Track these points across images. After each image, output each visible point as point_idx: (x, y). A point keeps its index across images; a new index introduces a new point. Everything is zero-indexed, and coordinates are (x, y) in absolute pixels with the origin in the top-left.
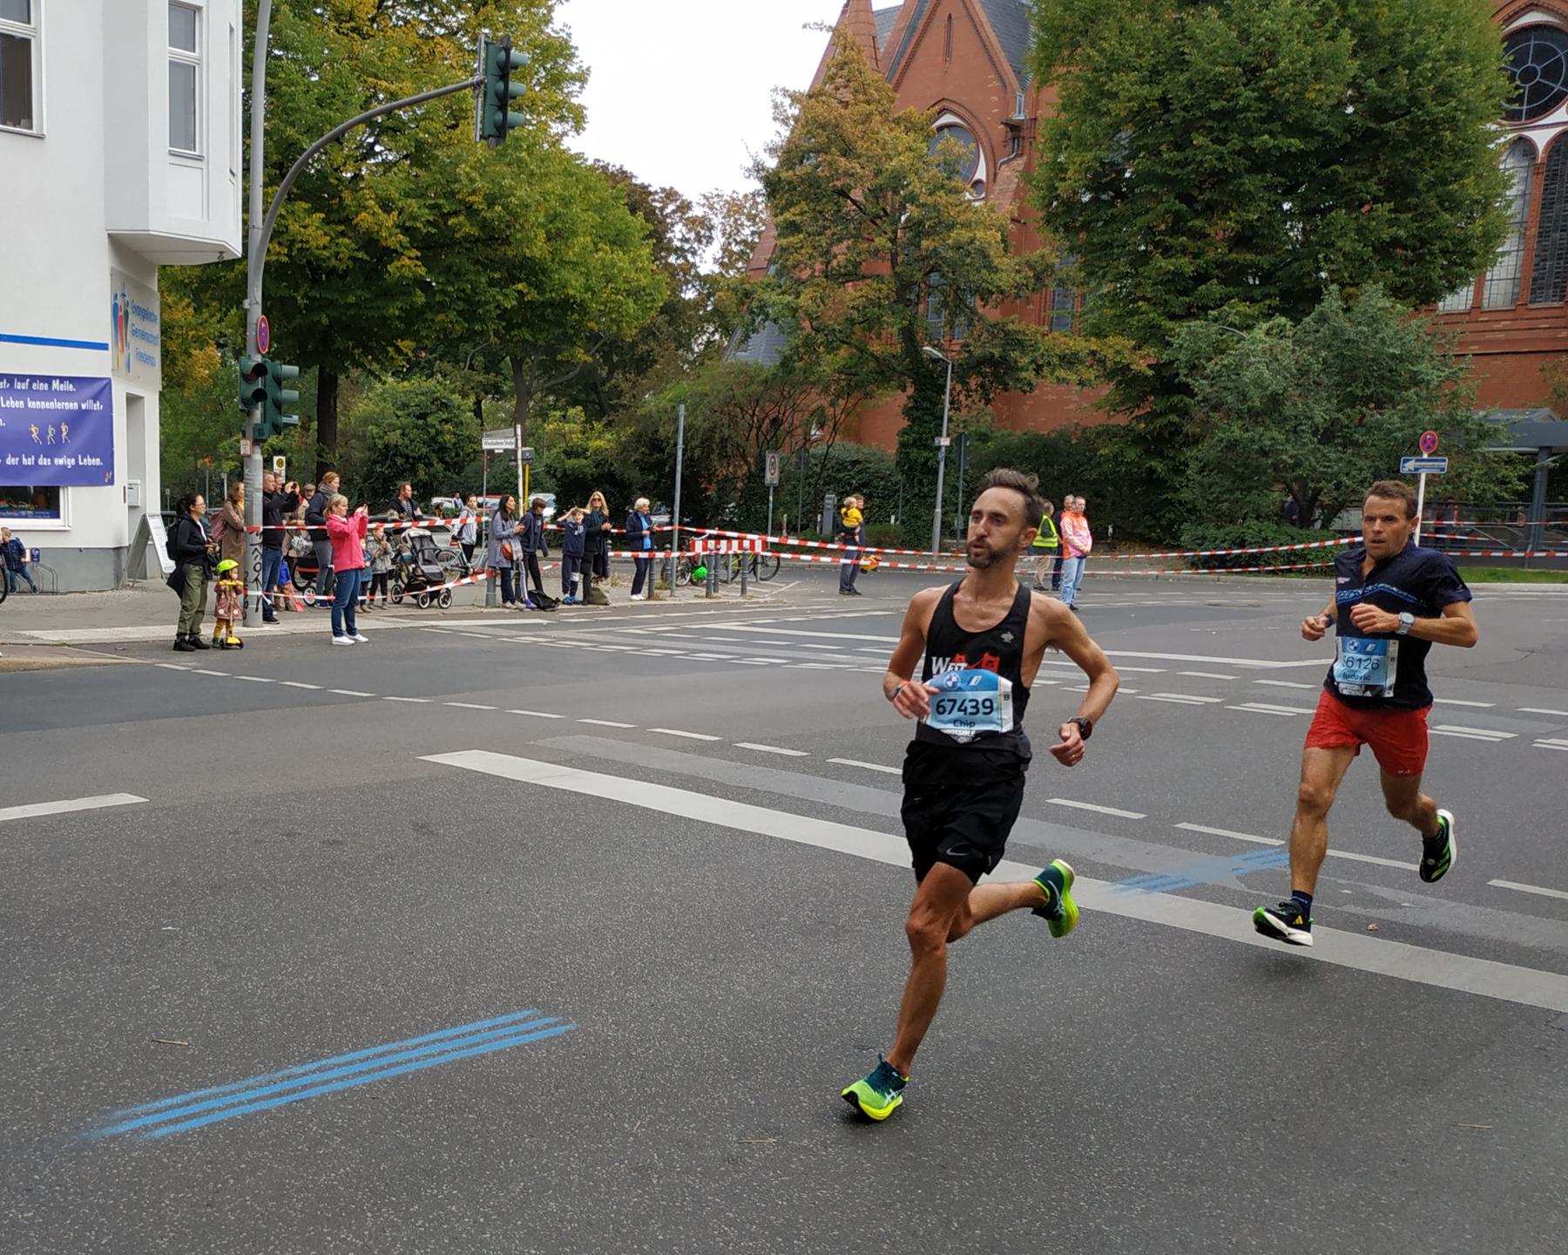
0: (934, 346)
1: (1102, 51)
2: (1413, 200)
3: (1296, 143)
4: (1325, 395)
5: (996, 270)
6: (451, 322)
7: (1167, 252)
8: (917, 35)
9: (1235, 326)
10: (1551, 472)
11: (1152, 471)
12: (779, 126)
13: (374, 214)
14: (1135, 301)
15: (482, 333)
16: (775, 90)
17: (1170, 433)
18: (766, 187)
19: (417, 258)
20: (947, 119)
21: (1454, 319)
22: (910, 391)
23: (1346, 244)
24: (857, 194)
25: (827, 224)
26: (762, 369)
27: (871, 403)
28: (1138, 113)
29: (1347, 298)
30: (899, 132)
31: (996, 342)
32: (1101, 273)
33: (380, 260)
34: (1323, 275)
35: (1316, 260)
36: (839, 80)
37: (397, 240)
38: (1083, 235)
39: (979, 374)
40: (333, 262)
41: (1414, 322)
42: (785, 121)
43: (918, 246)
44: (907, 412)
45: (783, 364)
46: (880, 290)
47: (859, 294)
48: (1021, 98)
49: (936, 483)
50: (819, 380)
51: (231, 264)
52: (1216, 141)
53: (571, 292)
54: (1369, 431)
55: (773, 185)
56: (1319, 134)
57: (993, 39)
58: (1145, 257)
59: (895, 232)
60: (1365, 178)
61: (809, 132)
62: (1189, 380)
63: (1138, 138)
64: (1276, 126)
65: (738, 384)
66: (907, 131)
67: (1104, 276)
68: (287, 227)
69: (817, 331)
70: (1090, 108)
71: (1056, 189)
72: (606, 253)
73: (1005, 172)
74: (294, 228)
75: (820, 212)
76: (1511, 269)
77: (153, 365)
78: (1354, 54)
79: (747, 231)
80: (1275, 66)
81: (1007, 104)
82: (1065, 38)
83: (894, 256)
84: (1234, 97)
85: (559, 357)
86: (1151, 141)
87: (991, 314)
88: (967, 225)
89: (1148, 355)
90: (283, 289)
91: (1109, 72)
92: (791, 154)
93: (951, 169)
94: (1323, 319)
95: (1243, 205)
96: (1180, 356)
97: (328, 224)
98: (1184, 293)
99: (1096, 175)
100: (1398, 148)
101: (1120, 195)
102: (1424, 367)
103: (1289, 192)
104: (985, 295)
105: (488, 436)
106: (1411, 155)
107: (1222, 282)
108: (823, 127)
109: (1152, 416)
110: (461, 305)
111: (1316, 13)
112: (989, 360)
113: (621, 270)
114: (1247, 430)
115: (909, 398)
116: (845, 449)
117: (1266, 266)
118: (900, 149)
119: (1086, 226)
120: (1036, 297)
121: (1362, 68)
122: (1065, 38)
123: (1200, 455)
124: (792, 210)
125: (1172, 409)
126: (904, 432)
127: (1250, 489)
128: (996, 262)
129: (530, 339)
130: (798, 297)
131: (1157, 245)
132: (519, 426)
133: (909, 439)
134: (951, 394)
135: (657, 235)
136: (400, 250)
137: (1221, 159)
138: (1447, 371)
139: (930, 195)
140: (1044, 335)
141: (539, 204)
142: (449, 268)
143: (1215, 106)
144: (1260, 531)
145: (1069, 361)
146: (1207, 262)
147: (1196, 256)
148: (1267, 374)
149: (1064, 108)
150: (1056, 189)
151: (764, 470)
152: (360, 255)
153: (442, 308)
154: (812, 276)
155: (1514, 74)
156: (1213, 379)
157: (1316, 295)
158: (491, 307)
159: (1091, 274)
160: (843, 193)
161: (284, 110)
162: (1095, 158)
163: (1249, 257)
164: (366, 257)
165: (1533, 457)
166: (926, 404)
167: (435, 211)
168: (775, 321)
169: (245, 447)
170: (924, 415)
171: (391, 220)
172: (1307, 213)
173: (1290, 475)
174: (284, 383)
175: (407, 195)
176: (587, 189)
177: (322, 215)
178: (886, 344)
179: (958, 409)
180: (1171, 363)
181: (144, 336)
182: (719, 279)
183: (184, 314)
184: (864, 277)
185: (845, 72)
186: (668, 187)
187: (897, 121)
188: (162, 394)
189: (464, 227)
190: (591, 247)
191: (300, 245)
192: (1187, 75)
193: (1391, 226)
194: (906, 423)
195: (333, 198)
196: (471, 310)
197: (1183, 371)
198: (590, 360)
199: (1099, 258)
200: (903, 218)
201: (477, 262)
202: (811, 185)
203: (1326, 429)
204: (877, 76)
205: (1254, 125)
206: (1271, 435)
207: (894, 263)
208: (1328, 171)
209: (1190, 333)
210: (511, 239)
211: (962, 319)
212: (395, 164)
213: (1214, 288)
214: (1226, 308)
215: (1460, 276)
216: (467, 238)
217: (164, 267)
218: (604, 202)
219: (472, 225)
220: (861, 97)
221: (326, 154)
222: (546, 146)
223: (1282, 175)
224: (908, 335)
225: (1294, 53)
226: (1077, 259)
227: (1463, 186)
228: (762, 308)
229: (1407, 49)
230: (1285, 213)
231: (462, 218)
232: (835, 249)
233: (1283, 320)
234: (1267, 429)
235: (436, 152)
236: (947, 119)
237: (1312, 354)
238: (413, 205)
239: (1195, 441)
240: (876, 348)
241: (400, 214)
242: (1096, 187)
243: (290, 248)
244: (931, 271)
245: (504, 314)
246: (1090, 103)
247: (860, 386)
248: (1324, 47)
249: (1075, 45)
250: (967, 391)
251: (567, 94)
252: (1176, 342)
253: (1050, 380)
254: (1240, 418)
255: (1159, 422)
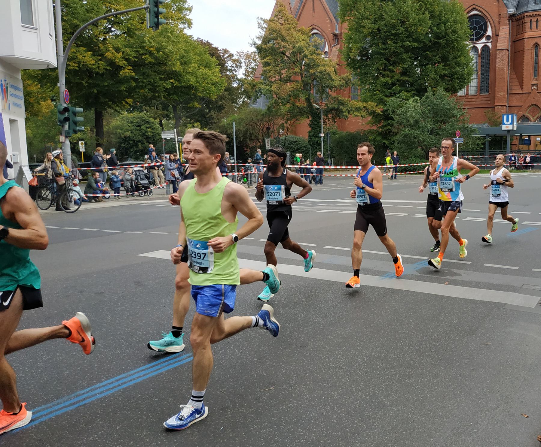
0: (317, 104)
1: (359, 13)
2: (449, 63)
3: (416, 45)
4: (430, 120)
5: (333, 80)
6: (146, 93)
7: (383, 76)
8: (303, 3)
9: (404, 99)
10: (489, 141)
11: (384, 143)
12: (260, 30)
13: (112, 53)
14: (375, 91)
15: (159, 97)
16: (258, 18)
17: (389, 132)
18: (257, 50)
19: (131, 69)
20: (315, 31)
21: (462, 98)
22: (310, 119)
23: (432, 75)
24: (288, 54)
25: (279, 63)
26: (261, 111)
27: (298, 122)
28: (372, 33)
29: (434, 91)
30: (299, 34)
31: (336, 103)
32: (365, 82)
33: (117, 69)
34: (427, 84)
35: (425, 80)
36: (279, 16)
37: (123, 63)
38: (359, 70)
39: (331, 113)
40: (97, 70)
41: (452, 99)
42: (262, 29)
43: (309, 72)
44: (310, 125)
45: (268, 109)
46: (298, 86)
47: (291, 87)
48: (337, 26)
49: (321, 148)
50: (281, 114)
51: (54, 69)
52: (394, 43)
53: (191, 83)
54: (442, 131)
55: (260, 49)
56: (422, 42)
57: (327, 7)
58: (377, 78)
59: (301, 67)
60: (436, 56)
61: (270, 33)
62: (393, 116)
63: (372, 41)
64: (411, 39)
65: (254, 116)
66: (303, 34)
67: (366, 82)
68: (77, 56)
69: (279, 99)
70: (357, 30)
71: (350, 55)
72: (203, 70)
73: (334, 49)
74: (80, 57)
75: (276, 59)
76: (475, 83)
77: (21, 107)
78: (430, 19)
79: (253, 65)
80: (409, 21)
81: (333, 27)
82: (348, 8)
83: (301, 75)
84: (398, 30)
85: (189, 106)
86: (376, 42)
87: (333, 94)
88: (323, 66)
89: (380, 108)
90: (77, 80)
91: (362, 20)
92: (266, 40)
93: (317, 47)
94: (428, 97)
95: (404, 63)
96: (390, 108)
97: (94, 56)
98: (389, 89)
99: (361, 51)
100: (443, 48)
101: (368, 58)
102: (455, 112)
103: (415, 59)
104: (331, 88)
105: (164, 133)
106: (447, 50)
107: (400, 86)
108: (275, 31)
109: (383, 126)
110: (150, 87)
111: (419, 6)
112: (334, 109)
113: (209, 76)
114: (410, 131)
115: (310, 121)
116: (291, 137)
117: (411, 81)
118: (300, 40)
119: (359, 67)
120: (346, 89)
121: (432, 23)
122: (348, 8)
123: (397, 139)
124: (267, 58)
125: (389, 125)
126: (310, 132)
127: (412, 149)
128: (333, 77)
129: (177, 99)
130: (271, 86)
131: (380, 74)
132: (175, 130)
133: (311, 134)
134: (323, 120)
135: (222, 65)
136: (124, 66)
137: (396, 48)
138: (461, 113)
139: (311, 55)
140: (350, 101)
141: (177, 52)
142: (144, 74)
143: (393, 32)
144: (416, 161)
145: (358, 109)
146: (395, 80)
147: (392, 77)
148: (414, 114)
149: (350, 30)
150: (350, 55)
151: (265, 144)
152: (108, 68)
153: (142, 87)
154: (275, 80)
155: (471, 28)
156: (399, 115)
157: (425, 90)
158: (161, 88)
159: (362, 82)
160: (284, 53)
161: (73, 13)
162: (360, 46)
163: (406, 78)
164: (110, 69)
165: (484, 138)
166: (316, 123)
167: (137, 53)
168: (264, 95)
169: (62, 139)
170: (315, 126)
171: (120, 55)
172: (421, 66)
173: (422, 144)
174: (77, 114)
175: (125, 47)
176: (194, 48)
177: (91, 53)
178: (301, 103)
179: (326, 124)
180: (387, 110)
181: (16, 96)
182: (245, 80)
183: (35, 88)
184: (292, 81)
185: (281, 14)
186: (225, 49)
187: (299, 31)
188: (27, 120)
189: (148, 59)
190: (197, 68)
191: (83, 63)
192: (384, 22)
193: (443, 70)
194: (310, 129)
195: (95, 46)
196: (154, 89)
197: (391, 113)
198: (200, 106)
199: (364, 78)
200: (303, 63)
201: (155, 72)
202: (272, 50)
203: (431, 130)
204: (291, 16)
205: (405, 39)
206: (417, 132)
207: (302, 78)
208: (425, 53)
209: (391, 101)
210: (167, 64)
211: (324, 96)
212: (120, 35)
213: (397, 88)
214: (401, 94)
215: (462, 85)
216: (150, 63)
217: (25, 70)
218: (201, 52)
219: (152, 58)
220: (287, 22)
221: (91, 30)
222: (178, 32)
223: (413, 54)
224: (308, 100)
225: (413, 18)
226: (357, 78)
227: (461, 59)
228: (260, 90)
229: (443, 18)
230: (415, 65)
231: (147, 56)
232: (283, 72)
233: (417, 98)
234: (415, 130)
235: (136, 32)
236: (315, 31)
237: (426, 108)
238: (128, 50)
239: (396, 134)
240: (298, 104)
241: (123, 54)
242: (361, 55)
243: (79, 65)
244: (313, 80)
245: (166, 90)
246: (357, 28)
247: (294, 117)
248: (421, 16)
249: (352, 11)
250: (328, 119)
251: (185, 14)
252: (388, 104)
253: (353, 115)
254: (407, 127)
255: (385, 128)
